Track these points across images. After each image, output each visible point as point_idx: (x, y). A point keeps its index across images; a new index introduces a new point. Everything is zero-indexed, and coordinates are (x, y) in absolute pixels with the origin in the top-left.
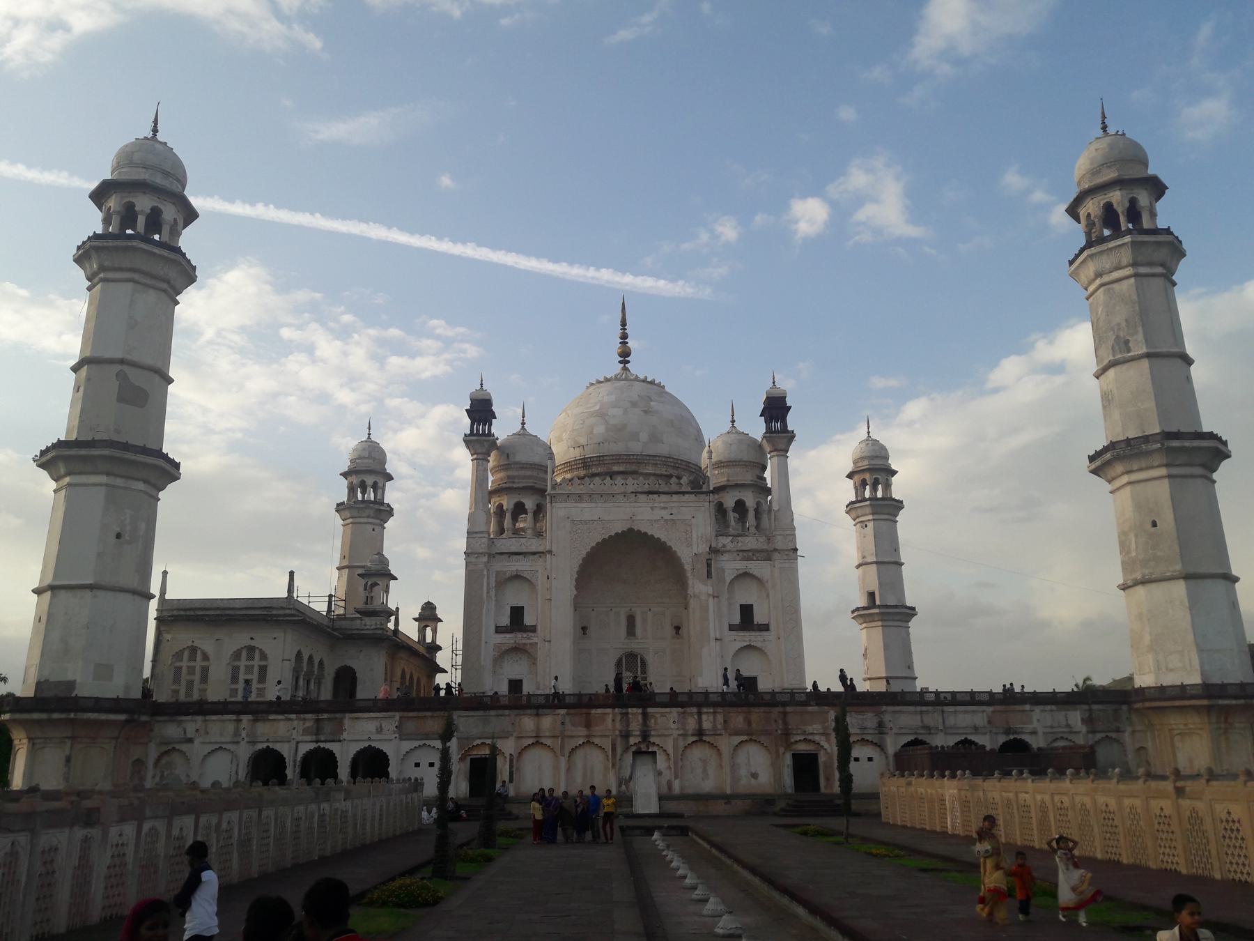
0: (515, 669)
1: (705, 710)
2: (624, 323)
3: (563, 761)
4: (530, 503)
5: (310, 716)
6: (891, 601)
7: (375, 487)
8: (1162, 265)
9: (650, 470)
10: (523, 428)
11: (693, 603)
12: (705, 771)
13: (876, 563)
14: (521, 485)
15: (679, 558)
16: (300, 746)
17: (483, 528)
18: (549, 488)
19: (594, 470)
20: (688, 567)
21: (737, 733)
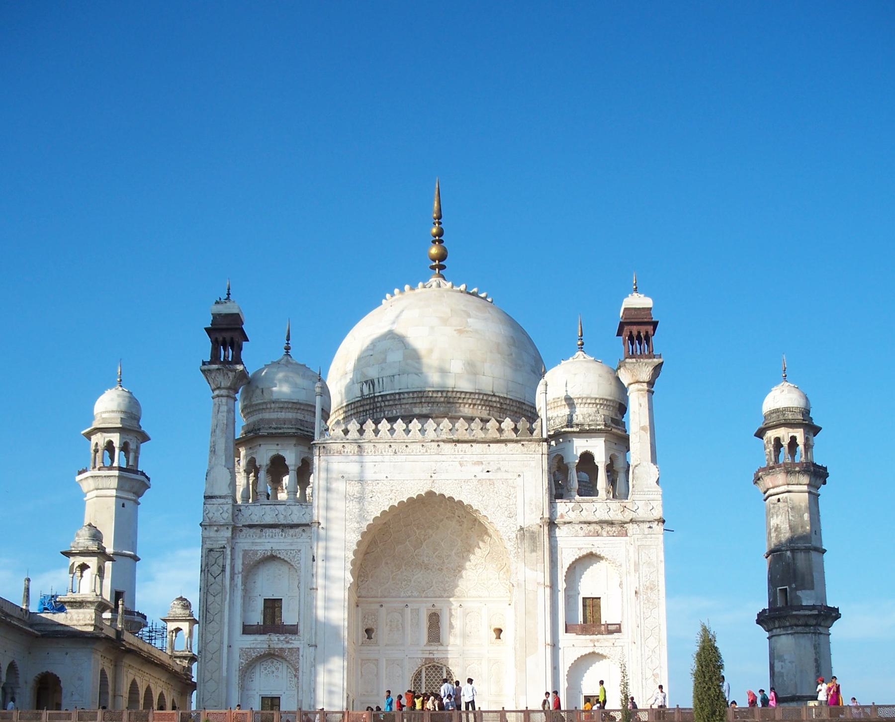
4: (291, 458)
7: (125, 448)
10: (287, 354)
17: (225, 491)
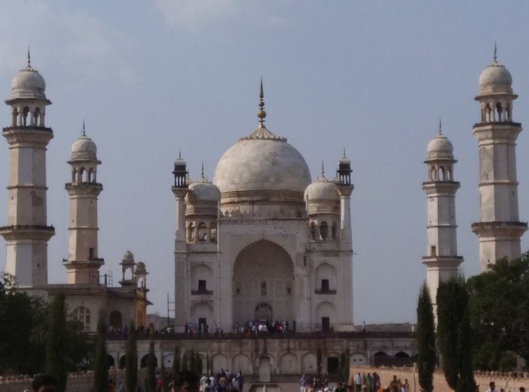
0: (202, 313)
1: (291, 340)
2: (262, 96)
3: (230, 362)
4: (207, 223)
5: (123, 341)
6: (446, 253)
8: (507, 138)
9: (275, 199)
11: (297, 280)
12: (290, 365)
13: (494, 184)
14: (203, 214)
15: (289, 256)
16: (120, 354)
17: (184, 239)
18: (218, 217)
19: (244, 199)
20: (294, 261)
21: (304, 349)
